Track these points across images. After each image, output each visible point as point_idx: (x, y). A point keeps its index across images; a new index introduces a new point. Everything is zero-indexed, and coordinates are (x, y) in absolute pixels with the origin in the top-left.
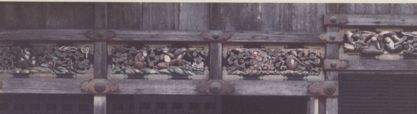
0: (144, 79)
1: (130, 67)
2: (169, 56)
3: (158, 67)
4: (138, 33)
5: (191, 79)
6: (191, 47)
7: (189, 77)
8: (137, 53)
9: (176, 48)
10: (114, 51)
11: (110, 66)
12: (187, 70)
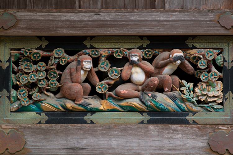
0: (85, 122)
1: (51, 95)
2: (143, 69)
4: (71, 17)
5: (194, 122)
6: (194, 48)
7: (189, 118)
8: (68, 63)
9: (157, 51)
10: (13, 59)
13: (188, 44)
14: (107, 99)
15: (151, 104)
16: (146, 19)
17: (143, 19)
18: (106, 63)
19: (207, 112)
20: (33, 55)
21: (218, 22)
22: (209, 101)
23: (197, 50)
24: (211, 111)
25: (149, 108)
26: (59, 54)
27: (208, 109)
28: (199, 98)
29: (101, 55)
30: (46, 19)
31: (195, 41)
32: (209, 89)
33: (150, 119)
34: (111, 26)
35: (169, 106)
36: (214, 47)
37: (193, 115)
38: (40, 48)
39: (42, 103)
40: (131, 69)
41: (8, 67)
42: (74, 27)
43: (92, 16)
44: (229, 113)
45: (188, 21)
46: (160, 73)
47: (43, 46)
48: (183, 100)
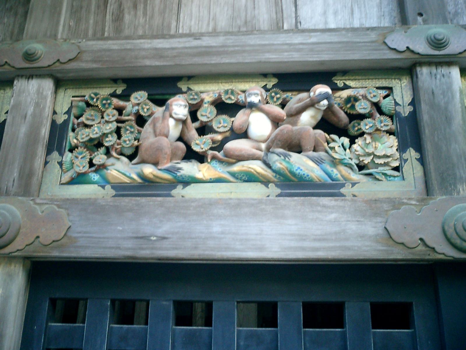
2: (268, 114)
3: (226, 155)
6: (346, 87)
9: (289, 94)
10: (74, 111)
11: (55, 155)
12: (335, 162)
13: (338, 82)
14: (209, 160)
15: (281, 166)
16: (271, 42)
17: (267, 42)
18: (209, 110)
19: (376, 182)
20: (102, 101)
21: (385, 43)
22: (377, 164)
23: (351, 90)
24: (381, 180)
25: (278, 176)
26: (139, 98)
27: (377, 177)
28: (361, 160)
29: (202, 101)
30: (123, 48)
31: (347, 78)
32: (377, 146)
33: (279, 193)
34: (218, 53)
35: (312, 171)
36: (377, 85)
37: (352, 187)
38: (114, 95)
39: (107, 169)
40: (249, 116)
41: (66, 122)
42: (161, 57)
43: (189, 41)
44: (413, 182)
45: (336, 43)
46: (294, 124)
47: (119, 92)
48: (335, 162)
